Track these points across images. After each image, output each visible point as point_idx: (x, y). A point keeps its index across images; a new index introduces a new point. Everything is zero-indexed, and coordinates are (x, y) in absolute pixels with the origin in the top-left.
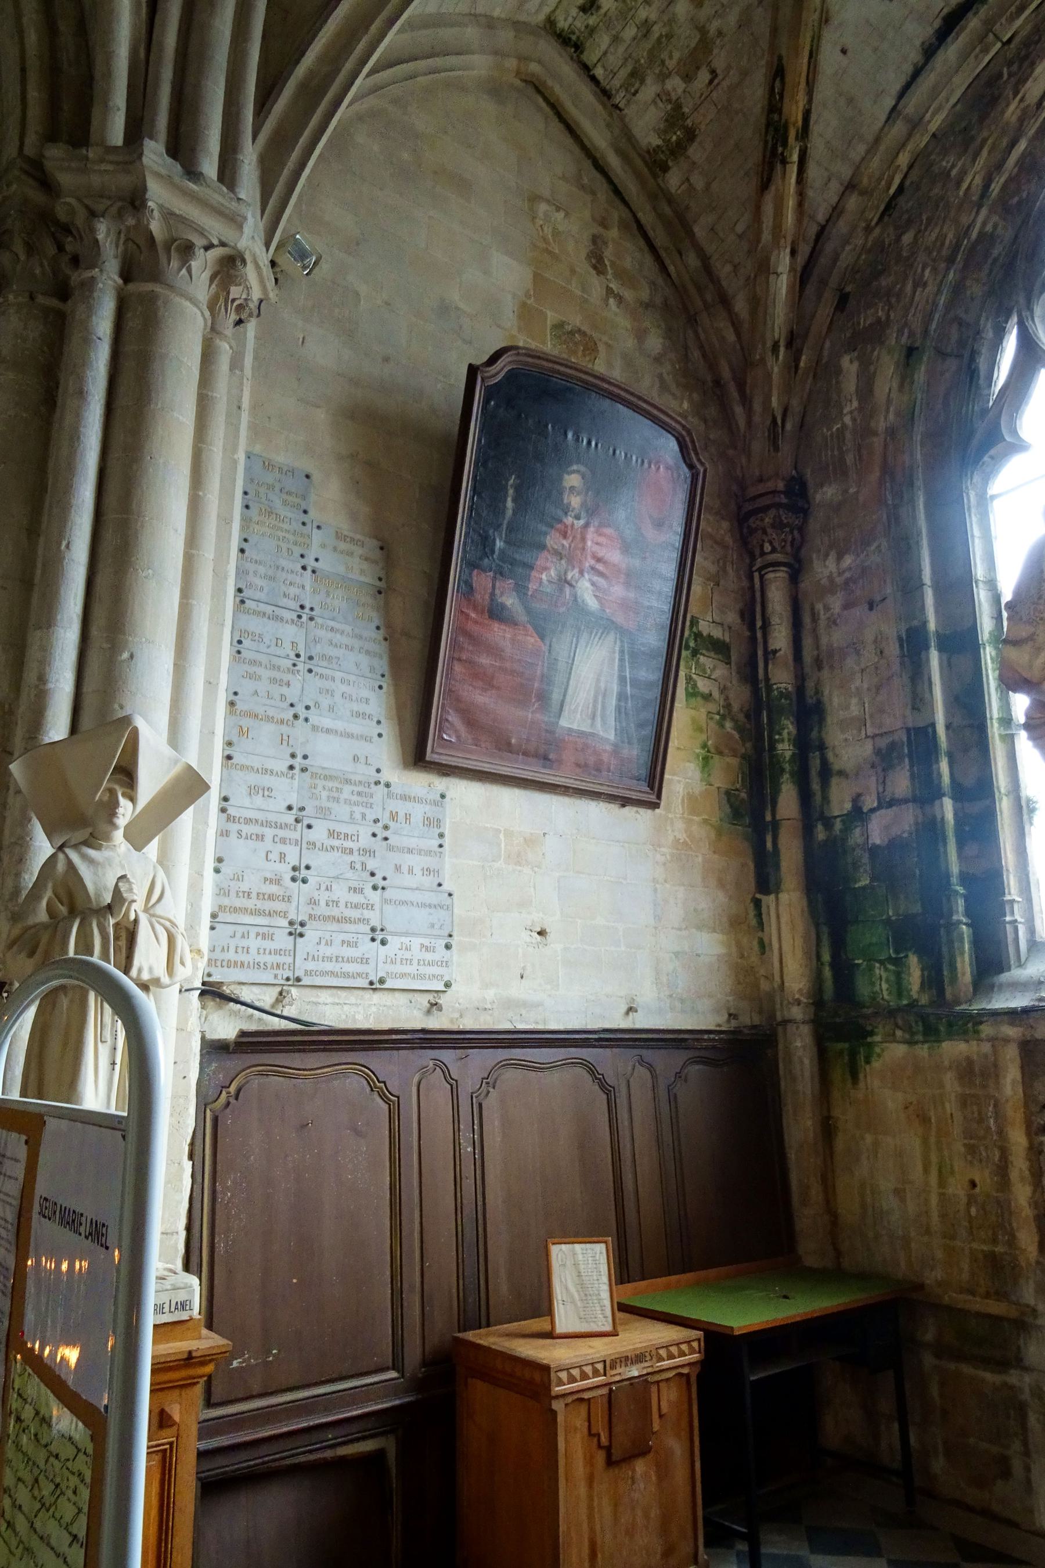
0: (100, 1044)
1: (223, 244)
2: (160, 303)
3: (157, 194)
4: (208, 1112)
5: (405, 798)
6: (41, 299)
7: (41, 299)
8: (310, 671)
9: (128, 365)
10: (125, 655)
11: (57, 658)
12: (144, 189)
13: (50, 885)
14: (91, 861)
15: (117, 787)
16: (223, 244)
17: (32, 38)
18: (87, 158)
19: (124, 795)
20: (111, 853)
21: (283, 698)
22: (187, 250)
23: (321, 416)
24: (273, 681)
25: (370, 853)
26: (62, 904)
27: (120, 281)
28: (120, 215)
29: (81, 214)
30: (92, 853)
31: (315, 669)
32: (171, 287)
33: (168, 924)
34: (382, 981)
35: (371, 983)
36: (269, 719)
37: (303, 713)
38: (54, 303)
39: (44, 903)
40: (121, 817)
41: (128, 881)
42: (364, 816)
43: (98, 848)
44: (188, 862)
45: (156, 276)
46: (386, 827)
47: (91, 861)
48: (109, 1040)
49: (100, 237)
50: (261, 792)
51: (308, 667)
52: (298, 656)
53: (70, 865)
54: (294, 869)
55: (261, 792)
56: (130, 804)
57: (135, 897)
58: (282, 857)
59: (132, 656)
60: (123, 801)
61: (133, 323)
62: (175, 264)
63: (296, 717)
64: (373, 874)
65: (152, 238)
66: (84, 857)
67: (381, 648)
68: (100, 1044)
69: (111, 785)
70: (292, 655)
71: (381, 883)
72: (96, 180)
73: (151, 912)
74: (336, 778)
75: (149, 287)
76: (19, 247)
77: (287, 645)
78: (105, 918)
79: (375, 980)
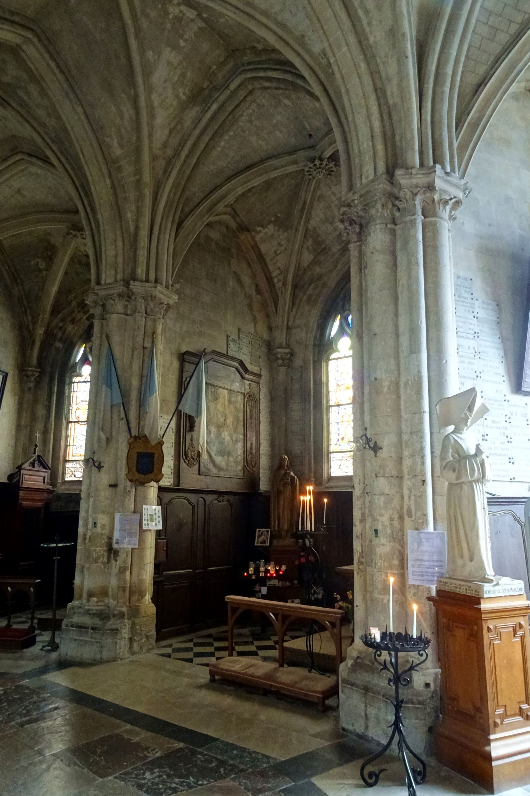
1: (455, 197)
2: (438, 225)
3: (439, 183)
5: (514, 406)
6: (389, 226)
7: (389, 226)
8: (480, 358)
9: (430, 250)
10: (444, 361)
12: (434, 182)
14: (461, 439)
16: (455, 197)
17: (377, 124)
18: (411, 173)
21: (472, 369)
22: (446, 202)
23: (472, 254)
24: (469, 363)
25: (504, 428)
27: (423, 217)
28: (424, 193)
29: (409, 195)
31: (481, 357)
32: (441, 218)
34: (514, 478)
35: (511, 479)
36: (469, 378)
37: (479, 375)
38: (392, 226)
39: (450, 454)
42: (502, 414)
43: (461, 433)
45: (435, 215)
46: (510, 418)
49: (416, 202)
51: (479, 356)
52: (476, 352)
53: (456, 441)
54: (483, 436)
58: (479, 431)
59: (446, 362)
61: (429, 234)
62: (441, 208)
63: (477, 376)
64: (507, 437)
65: (434, 200)
66: (458, 437)
67: (500, 346)
70: (474, 353)
71: (510, 440)
72: (414, 181)
74: (492, 399)
75: (434, 219)
76: (379, 206)
77: (472, 348)
79: (512, 478)
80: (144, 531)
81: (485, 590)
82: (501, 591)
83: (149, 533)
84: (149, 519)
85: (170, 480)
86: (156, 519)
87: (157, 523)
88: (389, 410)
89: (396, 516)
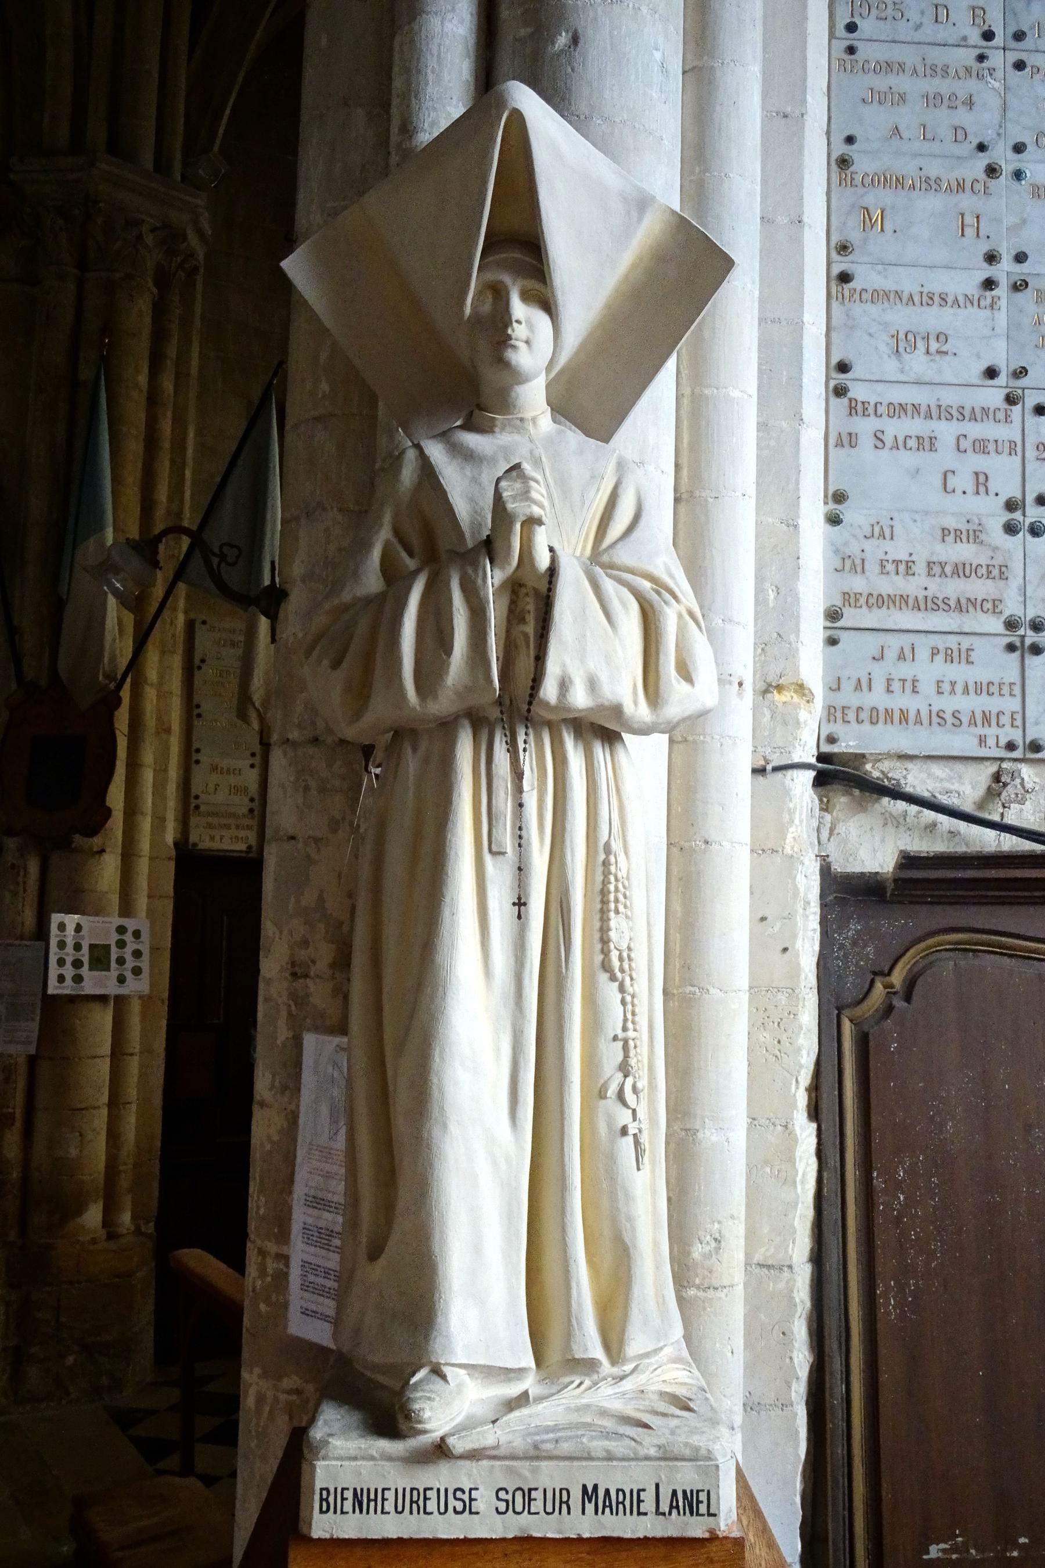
0: (488, 858)
4: (847, 1026)
8: (1020, 66)
10: (562, 40)
11: (431, 77)
13: (387, 519)
14: (467, 456)
15: (507, 279)
19: (527, 297)
20: (516, 437)
21: (959, 133)
24: (934, 100)
26: (411, 554)
30: (472, 440)
31: (1031, 60)
33: (646, 585)
36: (931, 184)
37: (1008, 162)
39: (376, 553)
40: (522, 345)
41: (524, 478)
43: (484, 428)
44: (752, 490)
47: (467, 456)
48: (509, 849)
50: (921, 345)
51: (1012, 57)
52: (988, 36)
53: (428, 472)
54: (1011, 506)
55: (921, 345)
56: (542, 320)
57: (536, 511)
58: (981, 482)
59: (575, 40)
60: (519, 308)
63: (992, 171)
68: (488, 858)
69: (490, 276)
70: (975, 36)
73: (605, 558)
77: (962, 17)
78: (475, 564)
80: (72, 999)
81: (321, 1479)
82: (485, 1500)
83: (96, 1009)
84: (86, 960)
85: (242, 833)
86: (121, 961)
87: (128, 974)
88: (325, 386)
89: (324, 953)
